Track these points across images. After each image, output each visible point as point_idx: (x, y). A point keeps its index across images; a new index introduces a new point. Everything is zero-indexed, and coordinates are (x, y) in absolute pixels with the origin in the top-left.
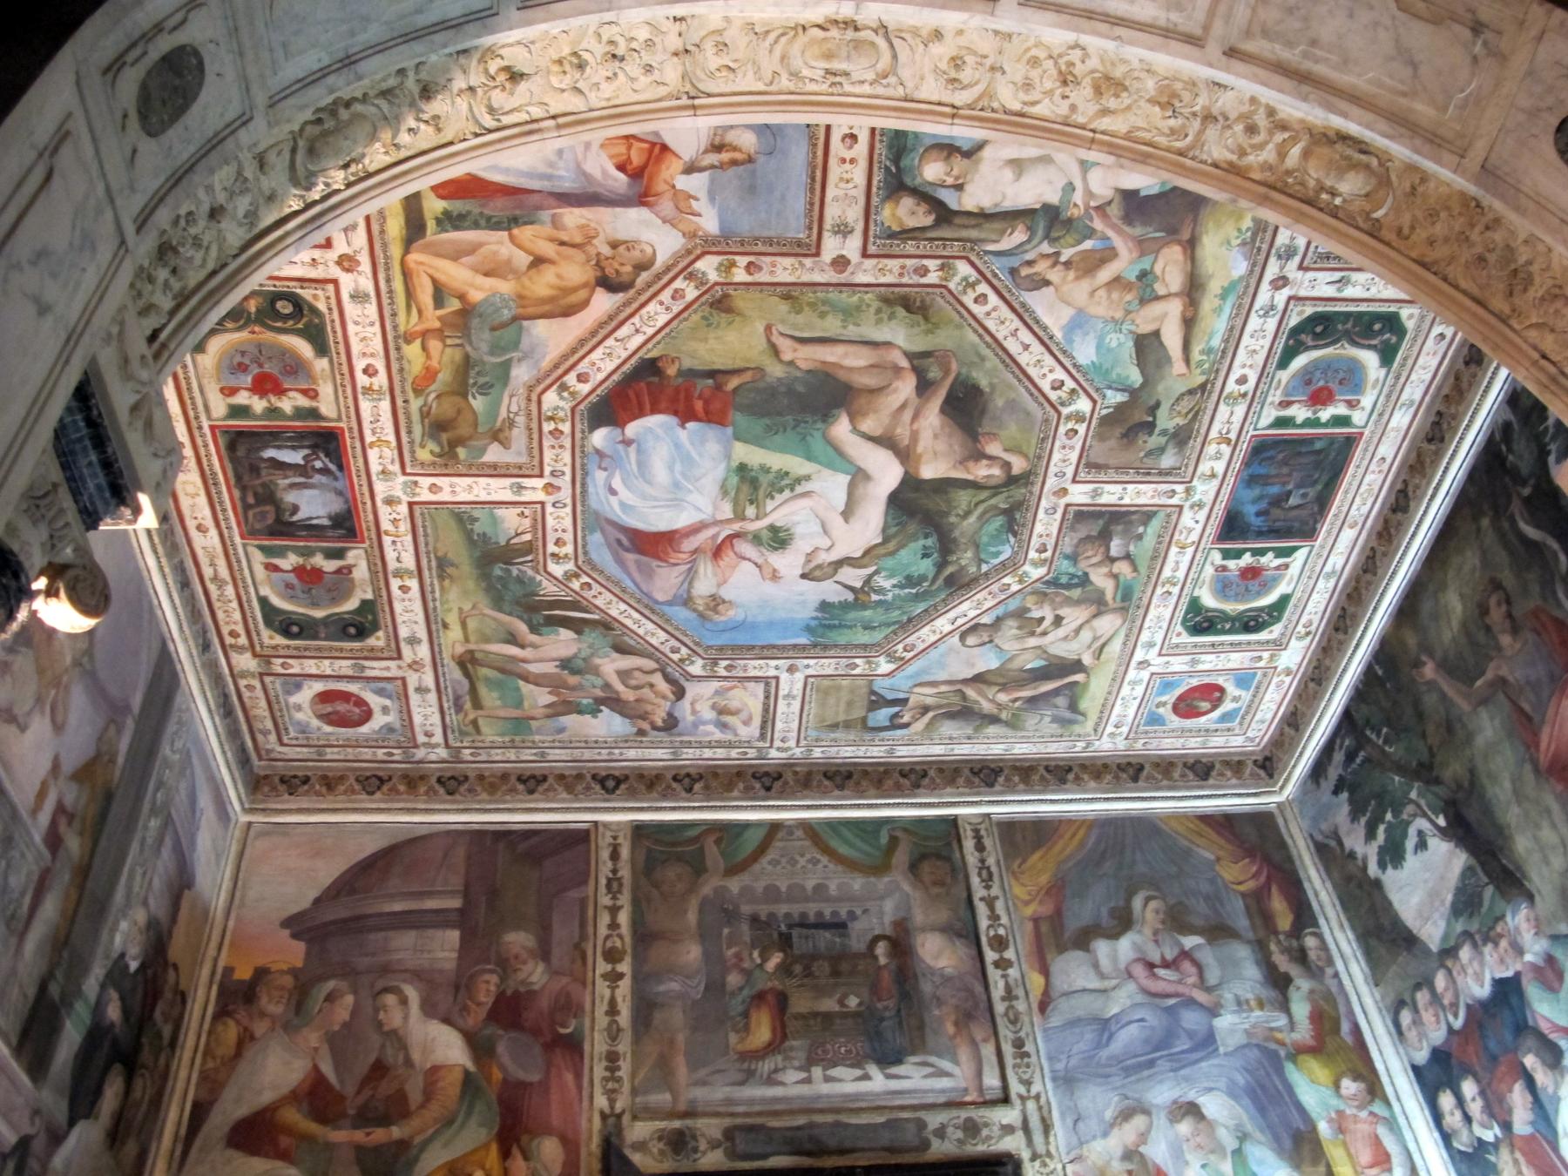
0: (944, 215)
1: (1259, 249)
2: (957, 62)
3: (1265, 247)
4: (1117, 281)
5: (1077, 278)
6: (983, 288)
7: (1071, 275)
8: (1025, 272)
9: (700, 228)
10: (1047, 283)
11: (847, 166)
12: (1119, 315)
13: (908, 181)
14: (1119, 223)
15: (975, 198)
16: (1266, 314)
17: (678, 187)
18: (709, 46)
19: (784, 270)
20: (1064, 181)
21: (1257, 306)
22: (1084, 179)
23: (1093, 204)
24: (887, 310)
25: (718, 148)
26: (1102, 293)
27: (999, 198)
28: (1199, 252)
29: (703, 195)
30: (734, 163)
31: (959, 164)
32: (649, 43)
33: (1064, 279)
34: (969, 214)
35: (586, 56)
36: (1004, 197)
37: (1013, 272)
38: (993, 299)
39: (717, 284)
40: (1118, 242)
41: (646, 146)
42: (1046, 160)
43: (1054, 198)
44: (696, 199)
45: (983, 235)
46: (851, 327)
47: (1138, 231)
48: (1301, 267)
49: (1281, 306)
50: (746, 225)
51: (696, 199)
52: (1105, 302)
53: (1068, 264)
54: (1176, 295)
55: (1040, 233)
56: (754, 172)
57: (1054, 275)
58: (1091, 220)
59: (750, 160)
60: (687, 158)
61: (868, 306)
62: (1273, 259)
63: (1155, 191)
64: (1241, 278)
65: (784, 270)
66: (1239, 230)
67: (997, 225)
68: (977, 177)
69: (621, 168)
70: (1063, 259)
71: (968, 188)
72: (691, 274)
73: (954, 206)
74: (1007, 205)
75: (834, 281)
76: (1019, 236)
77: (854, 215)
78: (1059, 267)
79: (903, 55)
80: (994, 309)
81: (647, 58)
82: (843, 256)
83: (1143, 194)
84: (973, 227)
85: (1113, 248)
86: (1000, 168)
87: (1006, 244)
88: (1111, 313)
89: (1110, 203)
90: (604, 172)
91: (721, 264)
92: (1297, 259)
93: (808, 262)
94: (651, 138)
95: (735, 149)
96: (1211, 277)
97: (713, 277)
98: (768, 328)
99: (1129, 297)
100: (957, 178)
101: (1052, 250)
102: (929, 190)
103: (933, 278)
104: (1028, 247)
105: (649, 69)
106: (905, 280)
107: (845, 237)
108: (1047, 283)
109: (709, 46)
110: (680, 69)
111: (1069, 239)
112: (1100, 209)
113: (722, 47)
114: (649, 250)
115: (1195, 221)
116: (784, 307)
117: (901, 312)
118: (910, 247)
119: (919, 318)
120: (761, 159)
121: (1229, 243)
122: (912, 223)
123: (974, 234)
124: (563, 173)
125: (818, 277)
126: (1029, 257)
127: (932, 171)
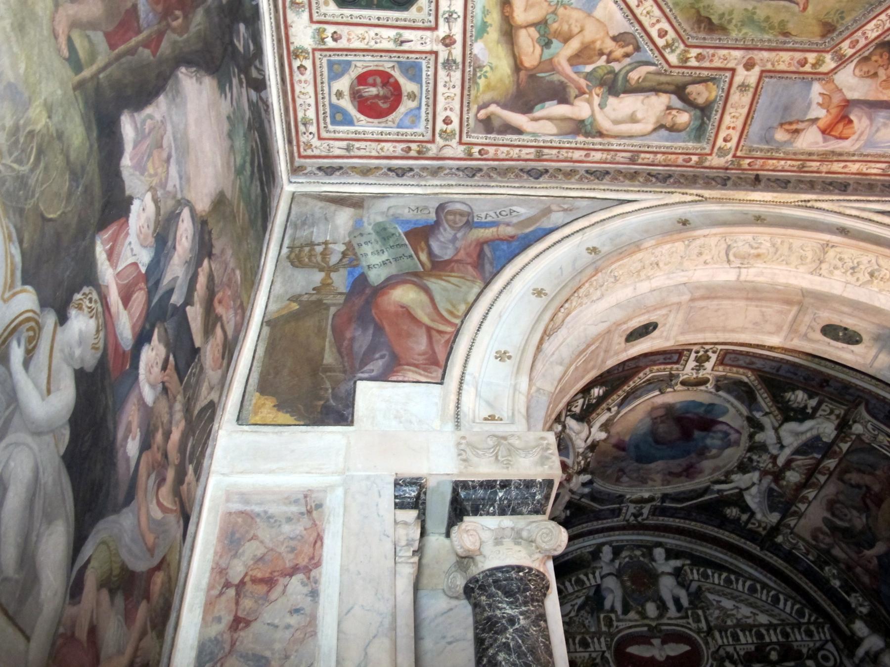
0: (680, 91)
1: (470, 66)
2: (701, 254)
3: (468, 69)
4: (566, 39)
5: (594, 42)
6: (661, 42)
7: (598, 45)
8: (630, 49)
9: (823, 86)
10: (614, 39)
11: (732, 125)
12: (561, 11)
13: (698, 113)
14: (569, 84)
15: (659, 102)
16: (451, 14)
17: (824, 111)
18: (808, 260)
19: (784, 60)
20: (606, 109)
21: (460, 21)
22: (593, 111)
23: (587, 96)
24: (724, 22)
25: (797, 132)
26: (576, 30)
27: (646, 101)
28: (511, 62)
29: (814, 106)
30: (790, 123)
31: (668, 121)
32: (836, 268)
33: (603, 42)
34: (666, 92)
35: (867, 276)
36: (643, 102)
37: (638, 48)
38: (654, 33)
39: (828, 52)
40: (568, 70)
41: (833, 133)
42: (616, 122)
43: (612, 100)
44: (819, 104)
45: (658, 78)
46: (750, 8)
47: (556, 78)
48: (436, 53)
49: (441, 21)
50: (796, 88)
51: (819, 104)
52: (572, 21)
53: (601, 54)
54: (521, 27)
55: (620, 78)
56: (782, 118)
57: (610, 45)
58: (587, 85)
59: (781, 125)
60: (815, 127)
61: (736, 26)
62: (459, 59)
63: (547, 104)
64: (476, 40)
65: (784, 60)
66: (486, 77)
67: (647, 84)
68: (658, 114)
69: (851, 122)
70: (604, 58)
71: (663, 107)
72: (840, 59)
73: (673, 97)
74: (640, 97)
75: (756, 52)
76: (635, 76)
77: (735, 97)
78: (607, 51)
79: (723, 253)
80: (653, 25)
81: (840, 264)
82: (748, 70)
83: (555, 102)
84: (662, 83)
85: (571, 65)
86: (644, 118)
87: (644, 70)
88: (567, 12)
89: (576, 97)
90: (860, 120)
91: (821, 65)
92: (441, 60)
93: (769, 67)
94: (829, 137)
95: (787, 131)
96: (498, 42)
97: (828, 57)
98: (805, 9)
99: (555, 26)
100: (670, 113)
101: (612, 64)
102: (687, 107)
103: (694, 52)
104: (628, 68)
105: (840, 259)
106: (711, 51)
107: (743, 83)
108: (614, 39)
109: (808, 260)
110: (826, 256)
111: (601, 72)
112: (584, 93)
113: (802, 258)
114: (857, 71)
115: (518, 85)
116: (790, 27)
117: (715, 20)
118: (705, 73)
119: (703, 13)
120: (775, 125)
121: (491, 68)
122: (700, 87)
123: (663, 79)
124: (882, 120)
125: (765, 54)
126: (628, 60)
127: (683, 118)
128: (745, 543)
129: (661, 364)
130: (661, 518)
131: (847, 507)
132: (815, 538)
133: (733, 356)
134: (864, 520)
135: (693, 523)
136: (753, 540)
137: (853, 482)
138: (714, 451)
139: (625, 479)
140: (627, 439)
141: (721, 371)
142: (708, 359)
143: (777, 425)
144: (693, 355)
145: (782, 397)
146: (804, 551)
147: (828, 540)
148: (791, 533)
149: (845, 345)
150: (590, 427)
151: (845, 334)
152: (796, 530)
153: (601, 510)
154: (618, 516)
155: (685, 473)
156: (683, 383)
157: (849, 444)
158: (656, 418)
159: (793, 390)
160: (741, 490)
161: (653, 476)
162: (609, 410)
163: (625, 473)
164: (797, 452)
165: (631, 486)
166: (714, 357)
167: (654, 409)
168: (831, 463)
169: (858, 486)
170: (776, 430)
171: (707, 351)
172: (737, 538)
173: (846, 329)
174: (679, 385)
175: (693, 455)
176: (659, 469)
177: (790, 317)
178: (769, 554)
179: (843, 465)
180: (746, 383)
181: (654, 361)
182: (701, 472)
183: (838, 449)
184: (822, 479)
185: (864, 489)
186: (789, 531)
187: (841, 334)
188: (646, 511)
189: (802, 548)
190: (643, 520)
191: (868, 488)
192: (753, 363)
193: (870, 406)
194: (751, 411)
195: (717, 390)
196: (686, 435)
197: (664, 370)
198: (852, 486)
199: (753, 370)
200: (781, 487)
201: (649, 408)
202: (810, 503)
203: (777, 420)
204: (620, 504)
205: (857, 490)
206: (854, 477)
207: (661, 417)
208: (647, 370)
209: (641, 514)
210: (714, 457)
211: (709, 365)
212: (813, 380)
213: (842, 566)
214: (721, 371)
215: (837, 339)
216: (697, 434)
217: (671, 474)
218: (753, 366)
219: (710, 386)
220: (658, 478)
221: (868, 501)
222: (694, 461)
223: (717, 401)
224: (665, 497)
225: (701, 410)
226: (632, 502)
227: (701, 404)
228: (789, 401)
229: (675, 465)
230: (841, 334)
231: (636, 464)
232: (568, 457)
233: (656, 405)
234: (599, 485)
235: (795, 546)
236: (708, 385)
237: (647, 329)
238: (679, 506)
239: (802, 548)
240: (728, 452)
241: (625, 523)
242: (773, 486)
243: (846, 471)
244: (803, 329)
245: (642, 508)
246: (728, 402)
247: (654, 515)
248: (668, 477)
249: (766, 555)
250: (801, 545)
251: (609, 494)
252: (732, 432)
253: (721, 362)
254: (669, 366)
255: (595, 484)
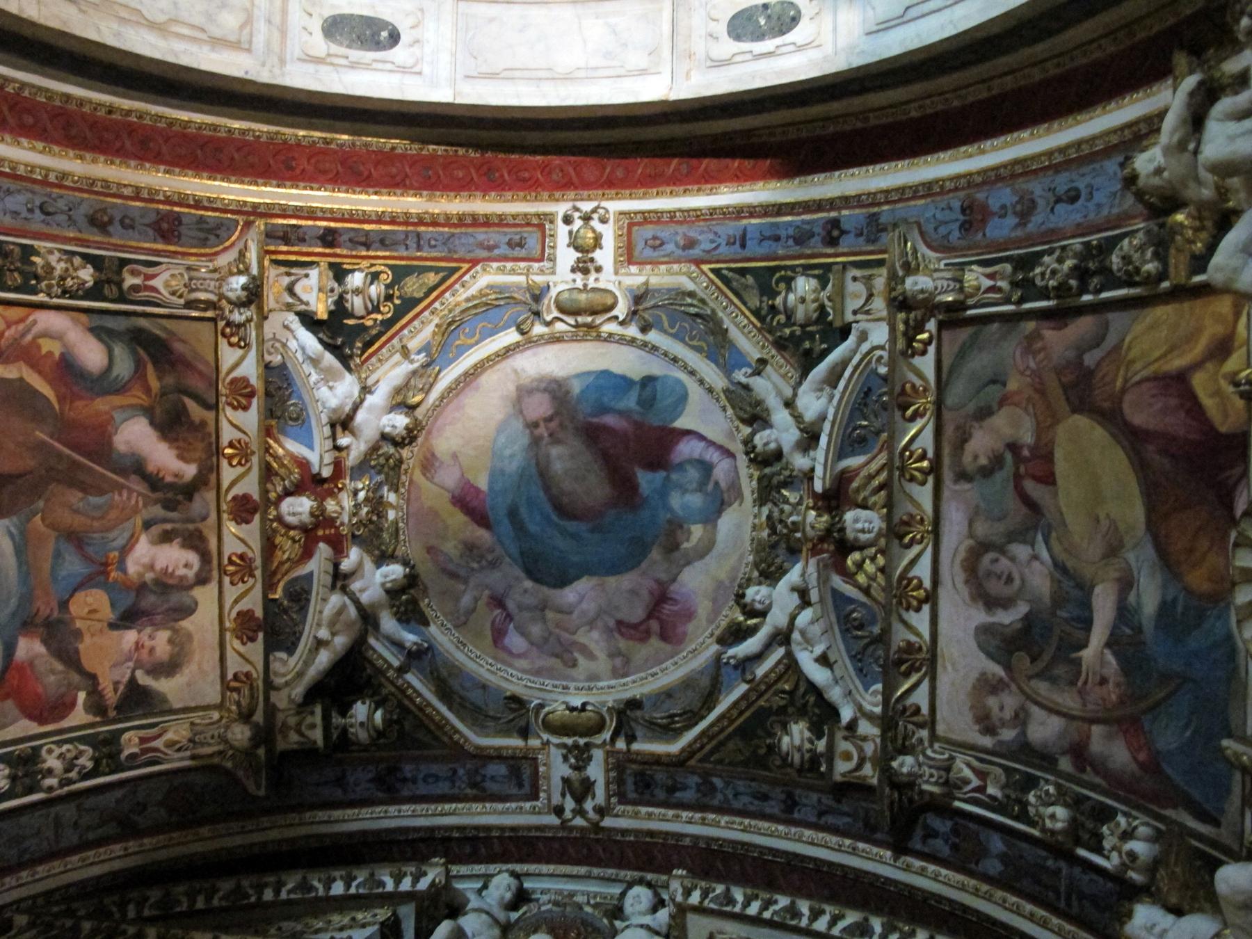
128: (854, 852)
129: (506, 259)
130: (644, 810)
131: (1002, 550)
132: (987, 724)
133: (649, 231)
134: (1045, 555)
135: (724, 819)
136: (868, 833)
137: (983, 461)
138: (697, 531)
139: (515, 641)
140: (483, 483)
141: (635, 278)
142: (597, 242)
143: (788, 392)
144: (562, 231)
145: (773, 308)
146: (976, 782)
147: (1009, 702)
148: (934, 737)
149: (779, 41)
150: (366, 390)
151: (769, 17)
152: (941, 729)
153: (485, 757)
154: (536, 797)
155: (654, 625)
156: (566, 309)
157: (932, 349)
158: (535, 425)
159: (789, 281)
160: (782, 637)
161: (582, 637)
162: (405, 352)
163: (509, 617)
164: (851, 442)
165: (538, 672)
166: (608, 233)
167: (524, 392)
168: (918, 434)
169: (997, 462)
170: (789, 404)
171: (587, 218)
172: (833, 840)
173: (765, 6)
174: (556, 314)
175: (655, 554)
176: (590, 606)
177: (666, 28)
178: (918, 863)
179: (949, 431)
180: (691, 294)
181: (490, 248)
182: (689, 615)
183: (918, 382)
184: (924, 495)
185: (1009, 457)
186: (924, 733)
187: (762, 22)
188: (596, 771)
189: (967, 773)
190: (602, 811)
191: (1013, 447)
192: (691, 244)
193: (929, 228)
194: (727, 370)
195: (644, 329)
196: (625, 491)
197: (513, 272)
198: (987, 472)
199: (698, 262)
200: (849, 576)
201: (511, 388)
202: (931, 598)
203: (784, 376)
204: (525, 733)
205: (999, 476)
206: (981, 444)
207: (549, 419)
208: (478, 268)
209: (587, 787)
210: (704, 550)
211: (605, 256)
212: (813, 235)
213: (1065, 764)
214: (635, 278)
215: (760, 36)
216: (646, 480)
217: (622, 626)
218: (696, 252)
219: (621, 311)
220: (593, 639)
221: (1029, 486)
222: (663, 576)
223: (656, 367)
224: (628, 715)
225: (630, 401)
226: (549, 727)
227: (624, 383)
228: (789, 314)
229: (624, 591)
230: (762, 22)
231: (528, 584)
232: (311, 447)
233: (525, 381)
234: (440, 635)
235: (952, 785)
236: (614, 313)
237: (373, 34)
238: (675, 748)
239: (967, 773)
240: (727, 522)
241: (553, 820)
242: (837, 581)
243: (963, 439)
244: (700, 46)
245: (581, 757)
246: (675, 360)
247: (623, 800)
248: (622, 644)
249: (908, 869)
250: (963, 768)
251: (484, 687)
252: (713, 456)
253: (628, 255)
254: (523, 264)
255: (433, 629)
